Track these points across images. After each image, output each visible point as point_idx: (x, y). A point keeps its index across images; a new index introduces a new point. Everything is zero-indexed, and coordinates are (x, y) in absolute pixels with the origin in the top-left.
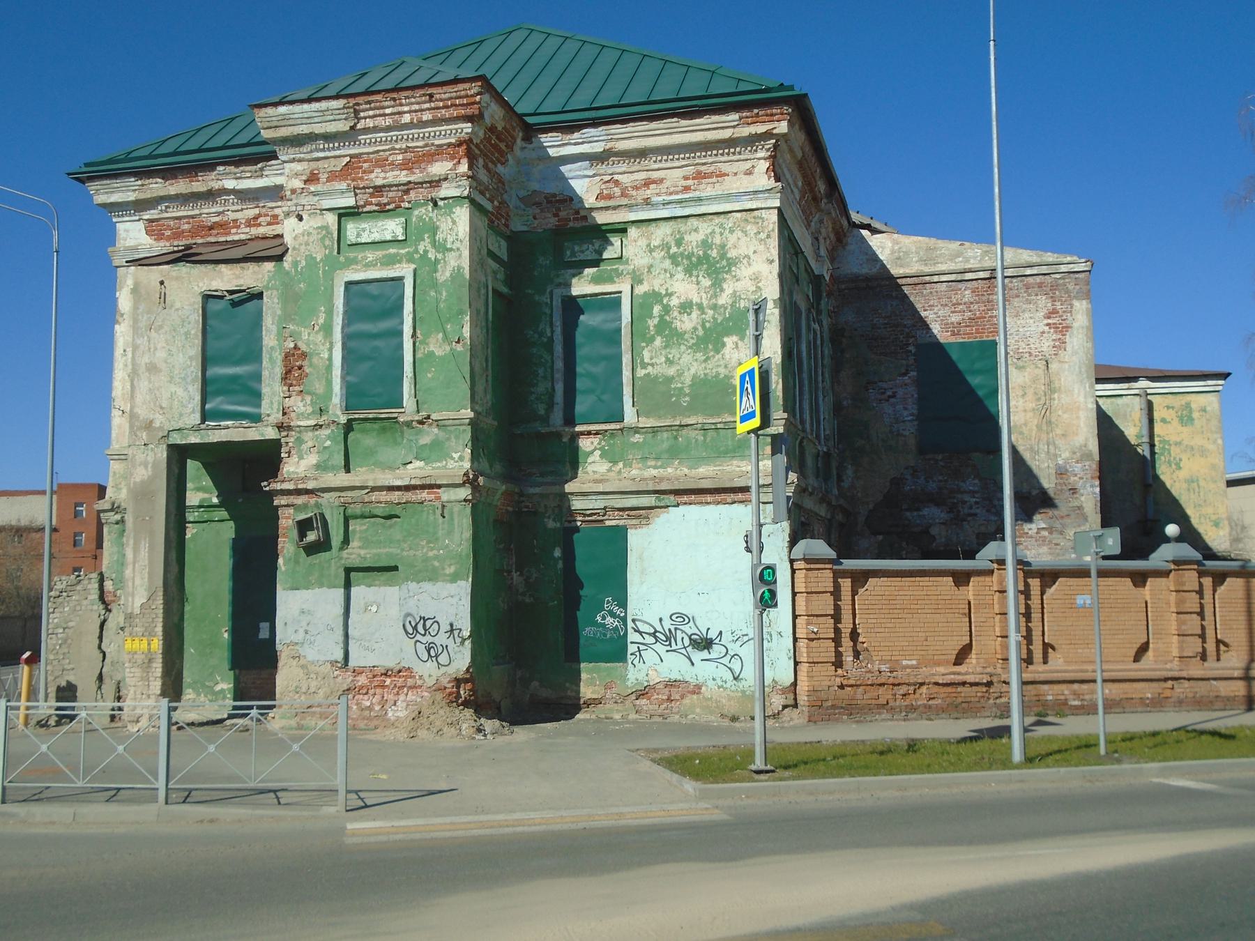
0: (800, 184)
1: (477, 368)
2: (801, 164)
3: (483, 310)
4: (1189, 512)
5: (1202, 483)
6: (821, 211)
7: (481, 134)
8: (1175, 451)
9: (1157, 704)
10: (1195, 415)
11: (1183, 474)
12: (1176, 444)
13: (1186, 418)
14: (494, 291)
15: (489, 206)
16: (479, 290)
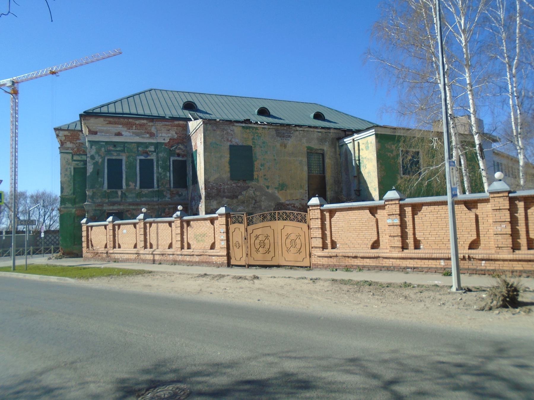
0: (120, 126)
1: (65, 186)
2: (110, 123)
3: (69, 173)
4: (369, 185)
5: (371, 173)
6: (152, 126)
7: (64, 138)
8: (365, 161)
9: (134, 261)
10: (369, 145)
11: (367, 170)
12: (365, 158)
13: (367, 148)
14: (74, 168)
15: (71, 151)
16: (67, 170)
